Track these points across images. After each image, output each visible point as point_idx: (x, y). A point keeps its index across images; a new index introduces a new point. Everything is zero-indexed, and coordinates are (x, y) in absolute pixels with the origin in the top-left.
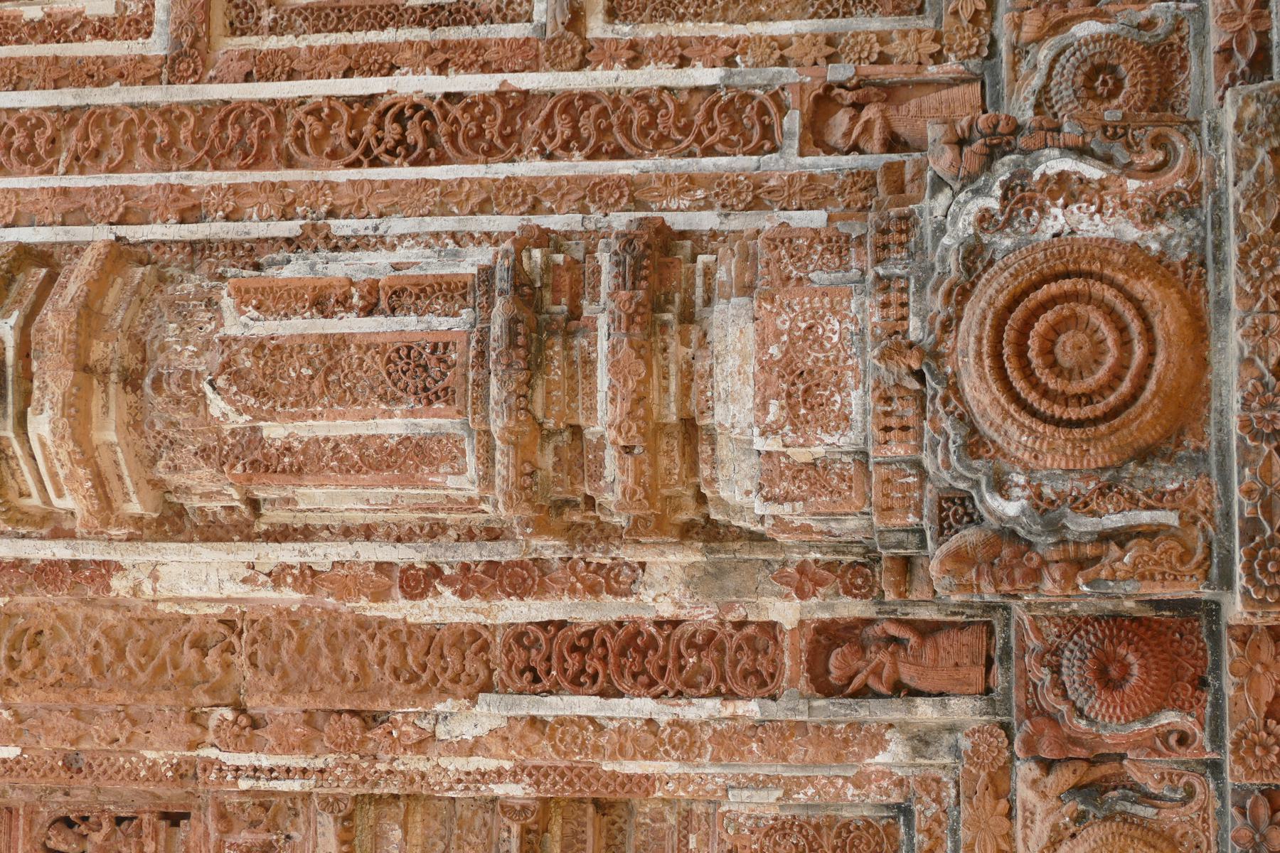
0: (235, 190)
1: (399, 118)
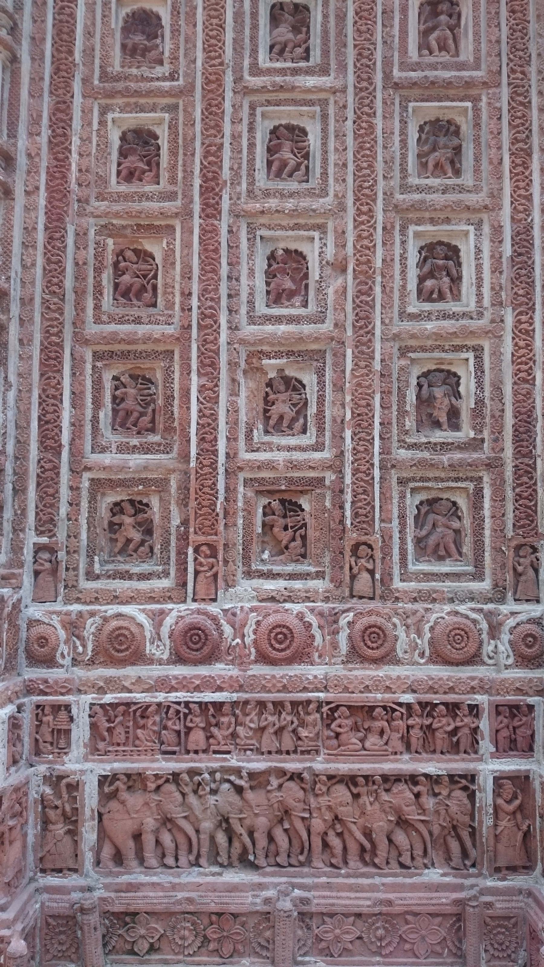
0: (30, 357)
1: (55, 411)
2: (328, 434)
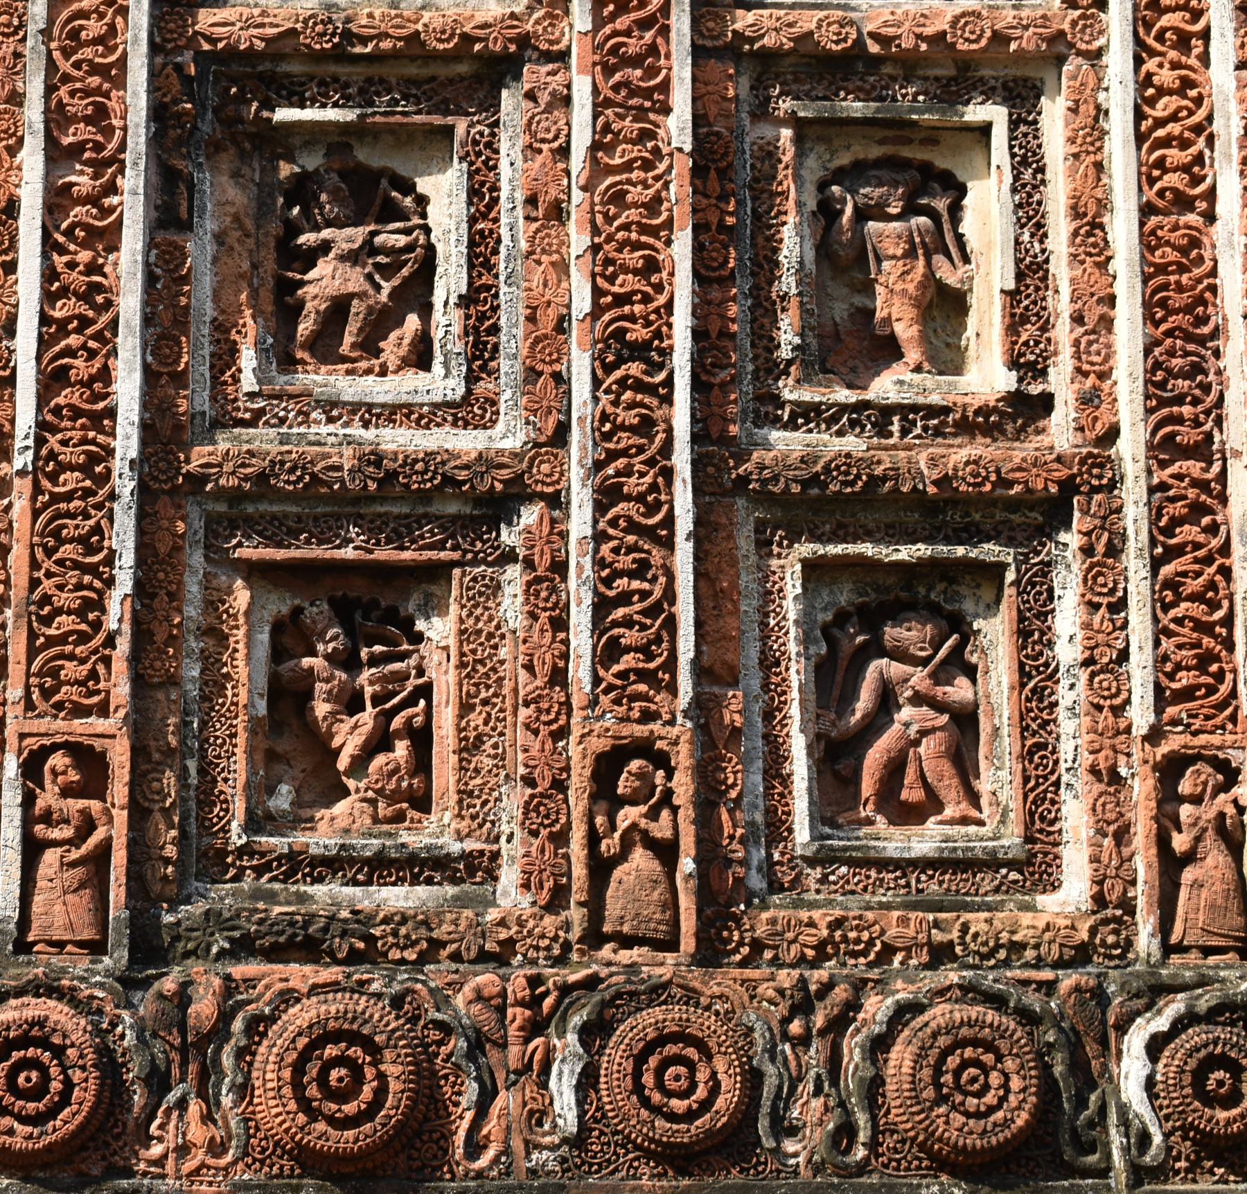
2: (508, 367)
